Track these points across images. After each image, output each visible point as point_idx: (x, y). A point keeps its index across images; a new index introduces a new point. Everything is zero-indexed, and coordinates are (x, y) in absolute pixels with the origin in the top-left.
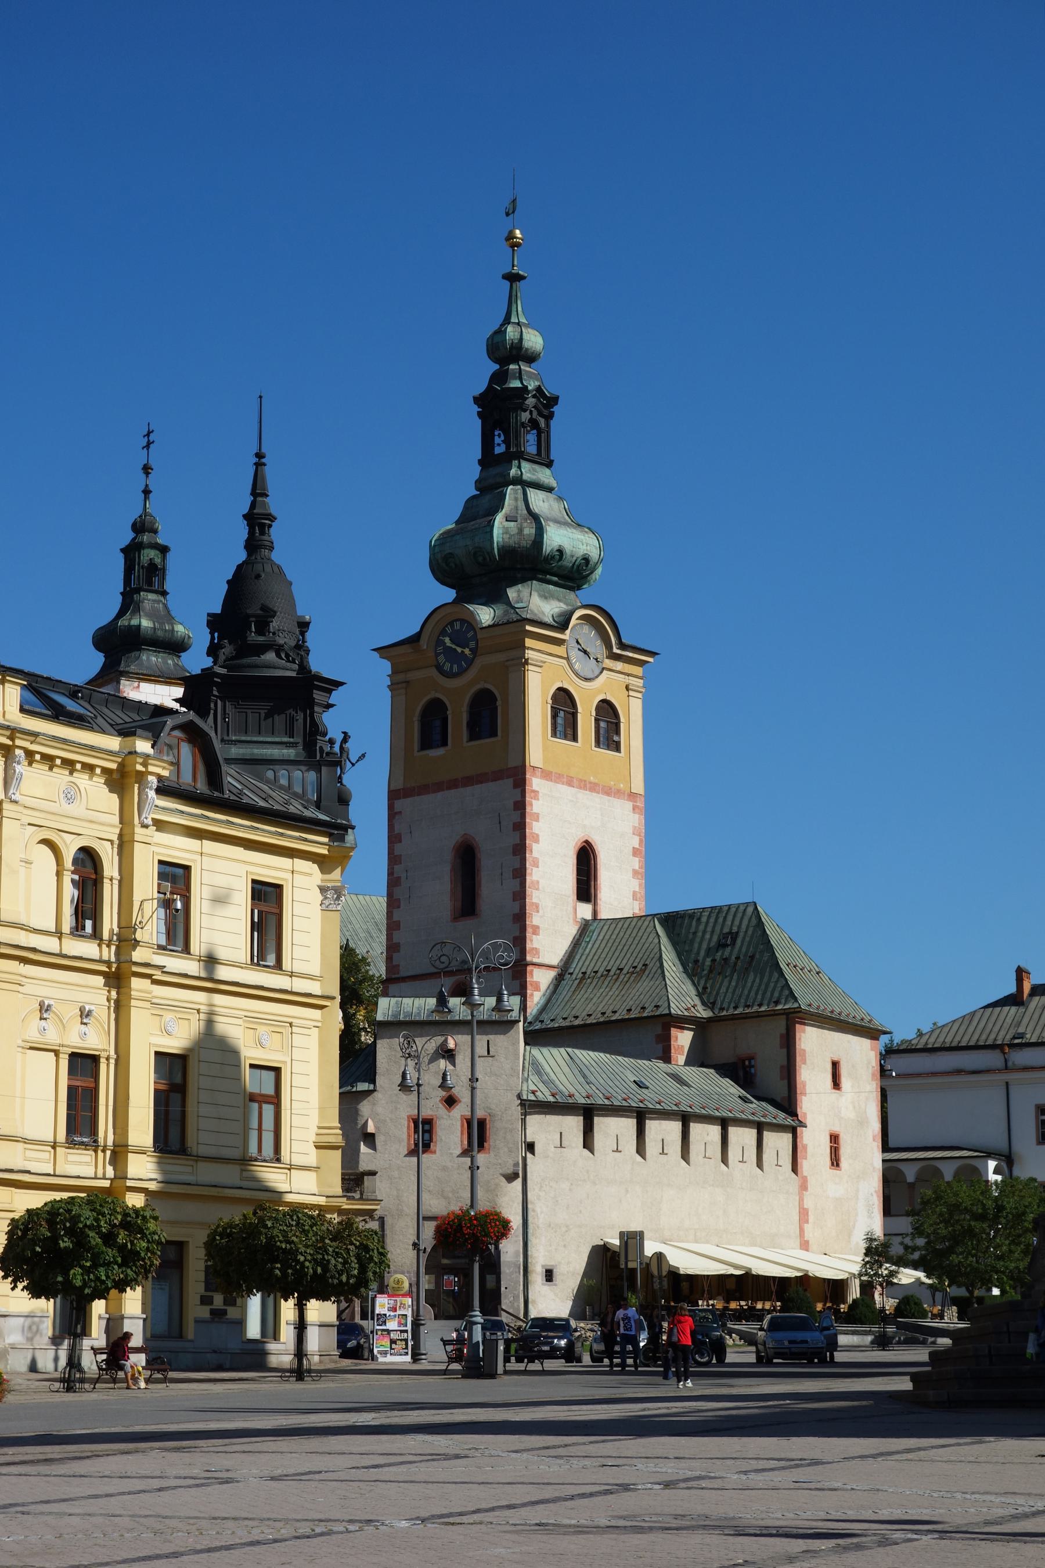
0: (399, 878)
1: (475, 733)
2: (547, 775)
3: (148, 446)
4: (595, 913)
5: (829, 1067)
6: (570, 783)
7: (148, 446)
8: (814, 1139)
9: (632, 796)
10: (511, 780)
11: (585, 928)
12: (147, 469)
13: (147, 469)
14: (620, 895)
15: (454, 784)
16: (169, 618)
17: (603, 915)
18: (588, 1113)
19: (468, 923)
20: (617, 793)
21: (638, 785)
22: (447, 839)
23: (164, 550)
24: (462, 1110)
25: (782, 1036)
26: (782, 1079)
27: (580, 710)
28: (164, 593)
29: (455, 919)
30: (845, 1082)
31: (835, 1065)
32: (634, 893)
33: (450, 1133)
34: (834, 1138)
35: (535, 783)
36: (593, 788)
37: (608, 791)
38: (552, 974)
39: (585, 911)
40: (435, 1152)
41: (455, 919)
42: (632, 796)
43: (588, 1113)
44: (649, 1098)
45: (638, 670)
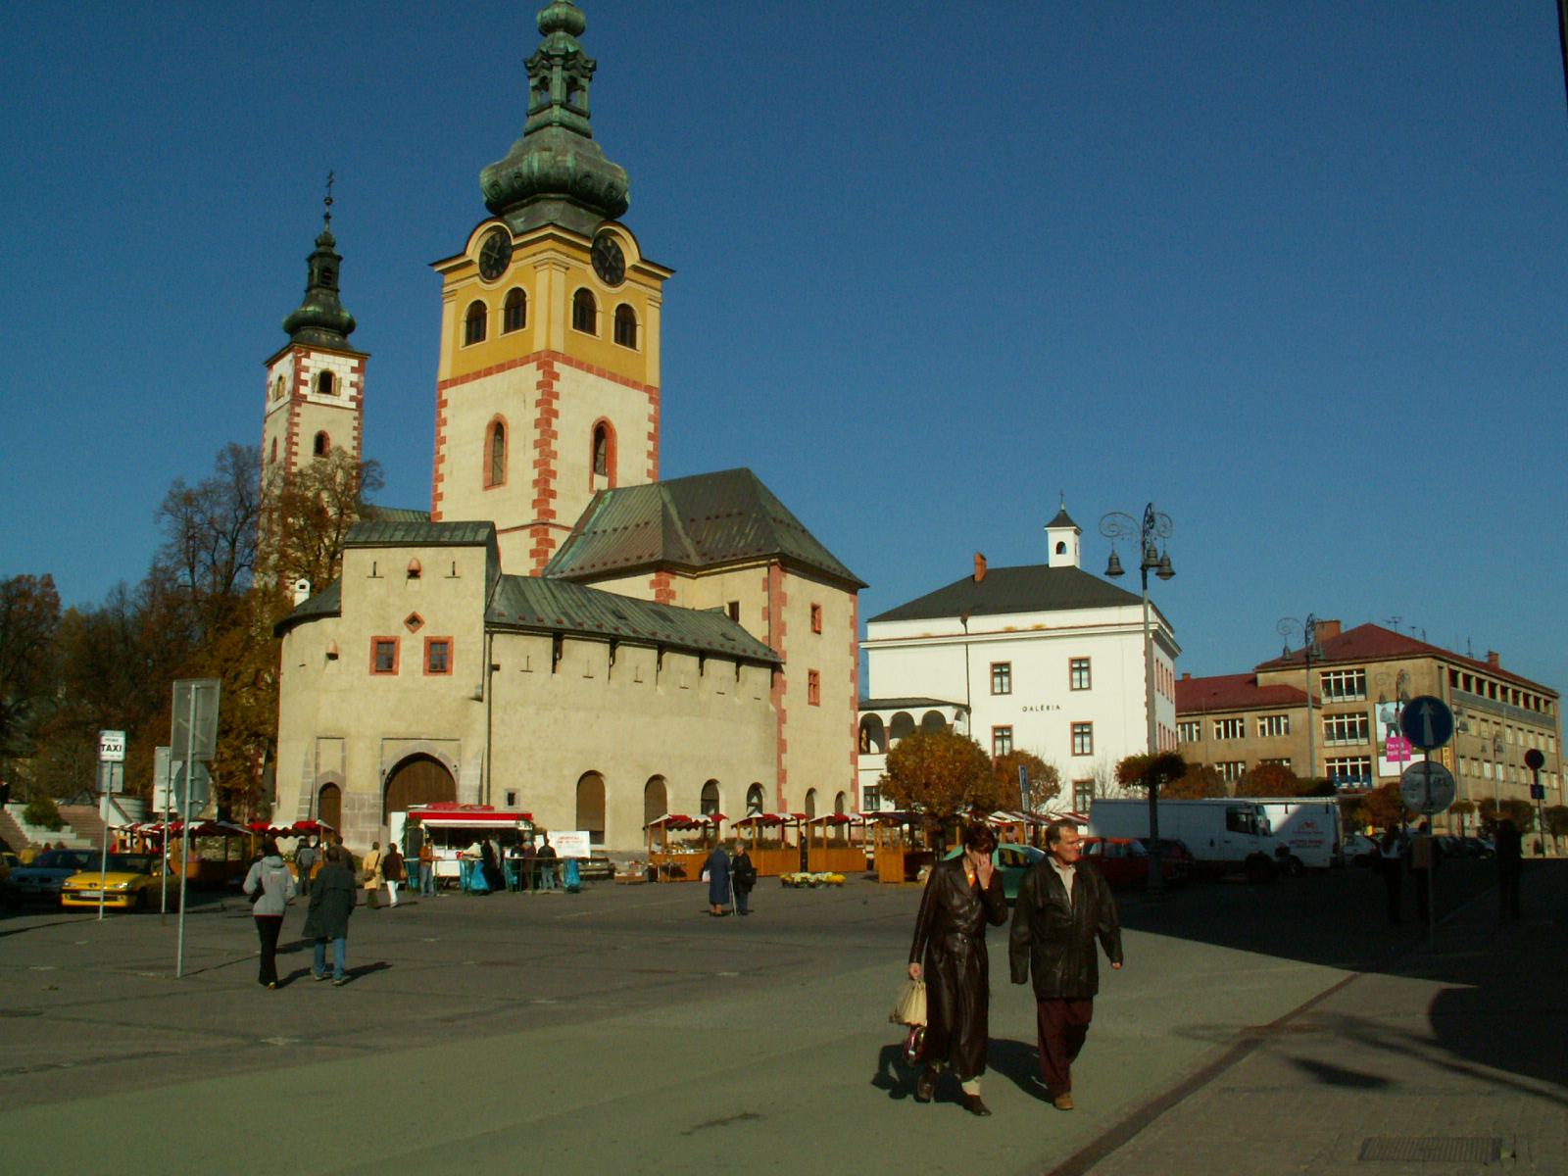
0: (443, 456)
1: (508, 328)
2: (568, 361)
3: (329, 185)
4: (612, 487)
5: (809, 611)
6: (589, 369)
7: (329, 185)
8: (795, 675)
9: (648, 389)
10: (535, 363)
11: (599, 496)
12: (329, 202)
13: (329, 202)
14: (634, 465)
15: (488, 372)
16: (337, 307)
17: (620, 484)
18: (558, 636)
19: (496, 491)
20: (635, 385)
21: (653, 377)
22: (485, 419)
23: (340, 258)
24: (425, 632)
25: (764, 579)
26: (764, 619)
27: (599, 307)
28: (338, 291)
29: (487, 488)
30: (825, 628)
31: (815, 608)
32: (648, 471)
33: (411, 653)
34: (813, 675)
35: (558, 367)
36: (613, 377)
37: (626, 382)
38: (568, 534)
39: (601, 482)
40: (397, 673)
41: (487, 488)
42: (648, 389)
43: (558, 636)
44: (625, 631)
45: (657, 284)
